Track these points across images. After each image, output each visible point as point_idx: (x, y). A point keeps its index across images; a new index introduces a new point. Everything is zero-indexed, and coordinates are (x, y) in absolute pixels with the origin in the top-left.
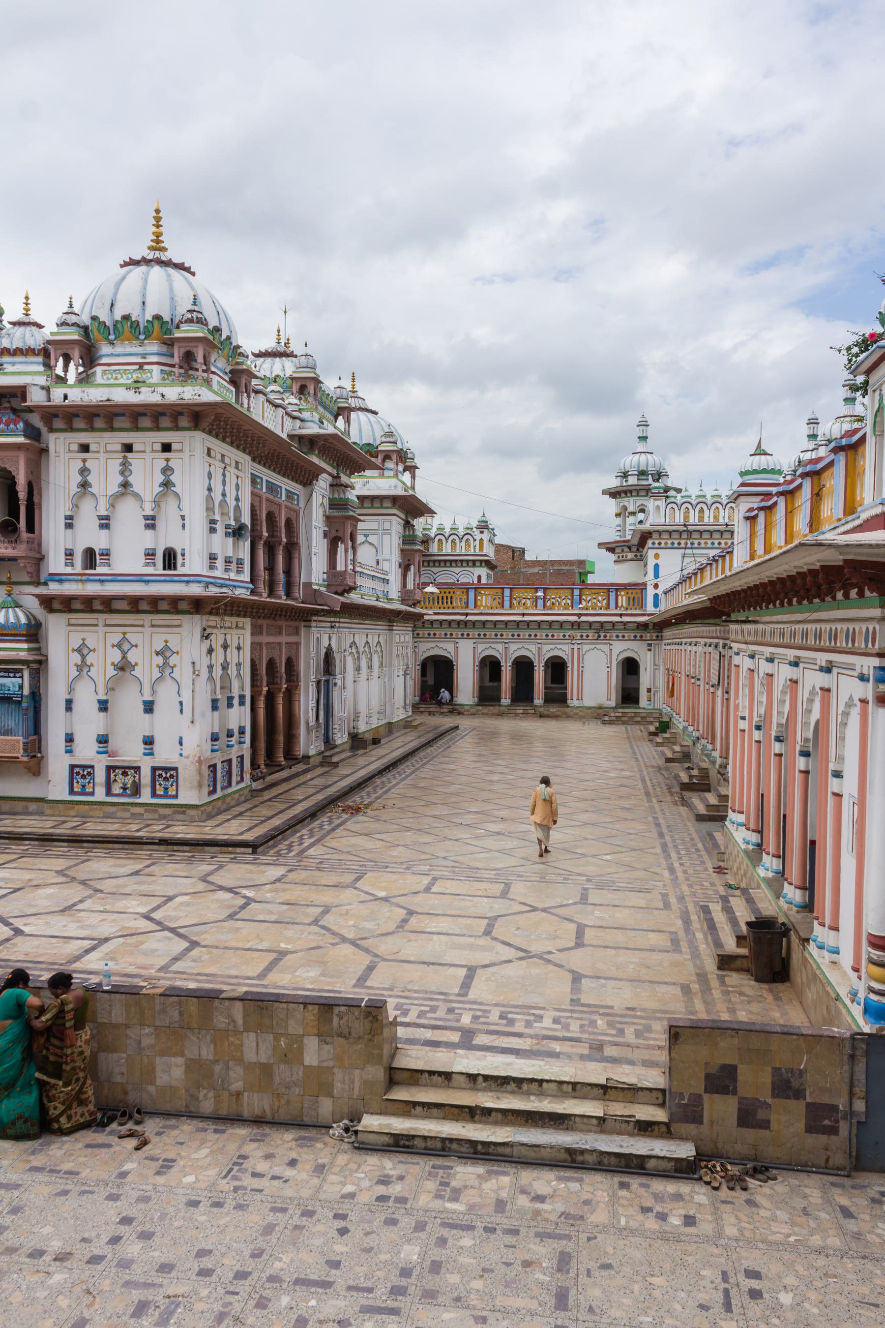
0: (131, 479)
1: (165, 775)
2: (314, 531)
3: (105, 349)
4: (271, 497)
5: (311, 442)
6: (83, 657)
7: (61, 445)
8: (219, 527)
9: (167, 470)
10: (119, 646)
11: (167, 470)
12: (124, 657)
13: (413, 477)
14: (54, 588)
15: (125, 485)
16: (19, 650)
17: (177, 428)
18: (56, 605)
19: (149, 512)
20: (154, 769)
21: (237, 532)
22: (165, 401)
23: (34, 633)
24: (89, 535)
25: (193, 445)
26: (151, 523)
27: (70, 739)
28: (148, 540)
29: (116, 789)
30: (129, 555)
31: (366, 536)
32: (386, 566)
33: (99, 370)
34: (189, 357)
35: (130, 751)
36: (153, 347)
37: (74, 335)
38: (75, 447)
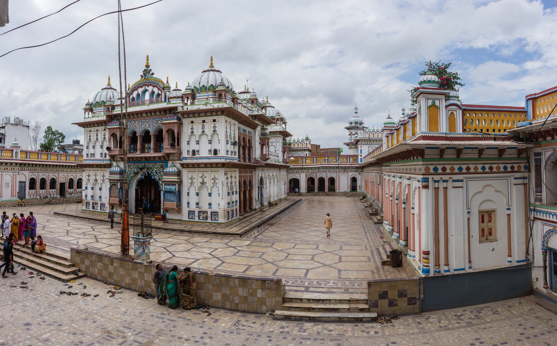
1: (215, 214)
3: (198, 95)
5: (255, 117)
6: (192, 180)
7: (186, 122)
8: (229, 142)
9: (215, 127)
10: (202, 177)
11: (215, 127)
13: (286, 125)
14: (184, 161)
15: (203, 132)
16: (175, 178)
17: (217, 115)
18: (185, 166)
19: (210, 139)
20: (212, 212)
21: (234, 144)
23: (179, 174)
24: (193, 146)
25: (222, 120)
26: (210, 142)
27: (188, 203)
28: (209, 147)
29: (201, 218)
30: (204, 151)
32: (278, 152)
33: (196, 101)
34: (220, 95)
35: (205, 207)
36: (211, 93)
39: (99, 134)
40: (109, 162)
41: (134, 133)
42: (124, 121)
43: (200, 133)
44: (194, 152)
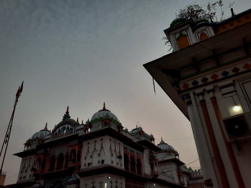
0: (96, 147)
2: (145, 162)
4: (132, 153)
8: (114, 155)
11: (102, 144)
12: (93, 185)
13: (178, 156)
15: (95, 149)
17: (103, 136)
19: (99, 153)
21: (120, 157)
22: (111, 138)
24: (89, 160)
25: (107, 138)
26: (99, 155)
31: (168, 169)
32: (173, 176)
37: (88, 124)
38: (87, 143)
39: (31, 161)
40: (34, 181)
41: (54, 156)
42: (48, 149)
43: (93, 150)
44: (89, 164)
